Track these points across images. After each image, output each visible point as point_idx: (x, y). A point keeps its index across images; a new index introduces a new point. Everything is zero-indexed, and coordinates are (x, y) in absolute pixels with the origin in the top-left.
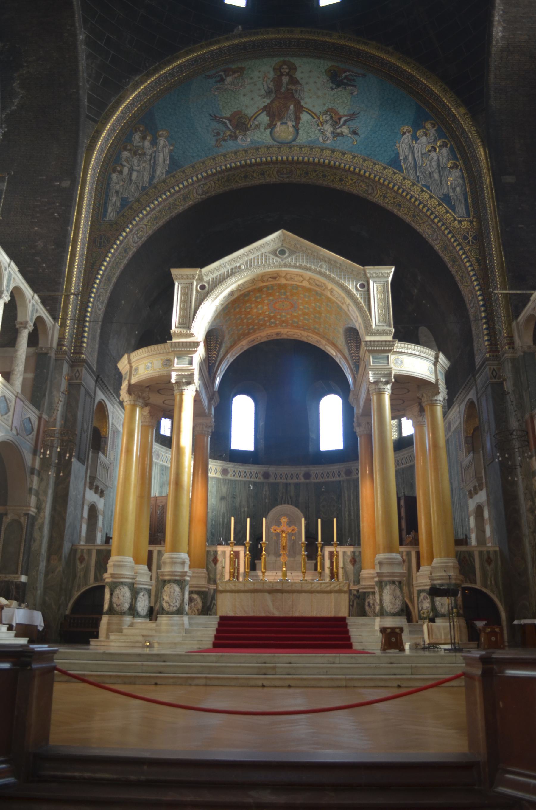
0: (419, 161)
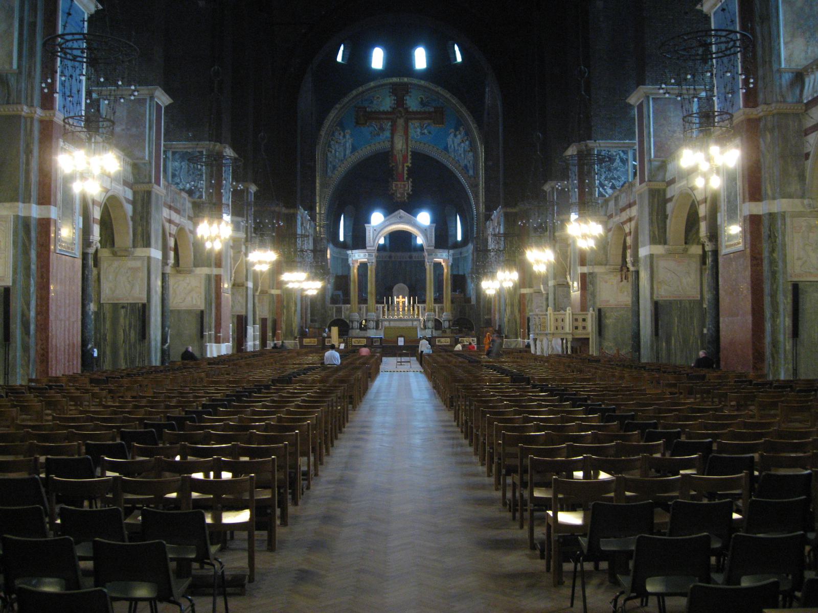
0: (456, 148)
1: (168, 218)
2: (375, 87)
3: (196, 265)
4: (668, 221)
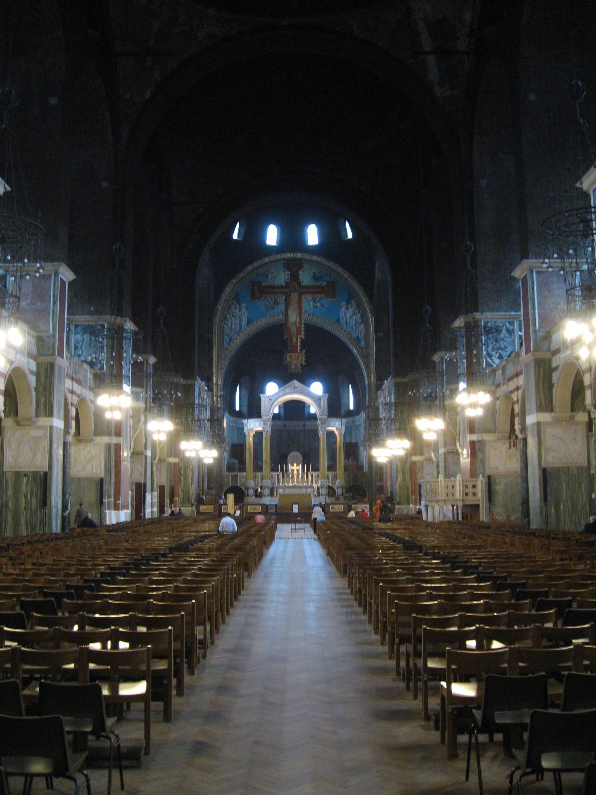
1: (70, 388)
2: (270, 262)
3: (95, 435)
4: (554, 390)
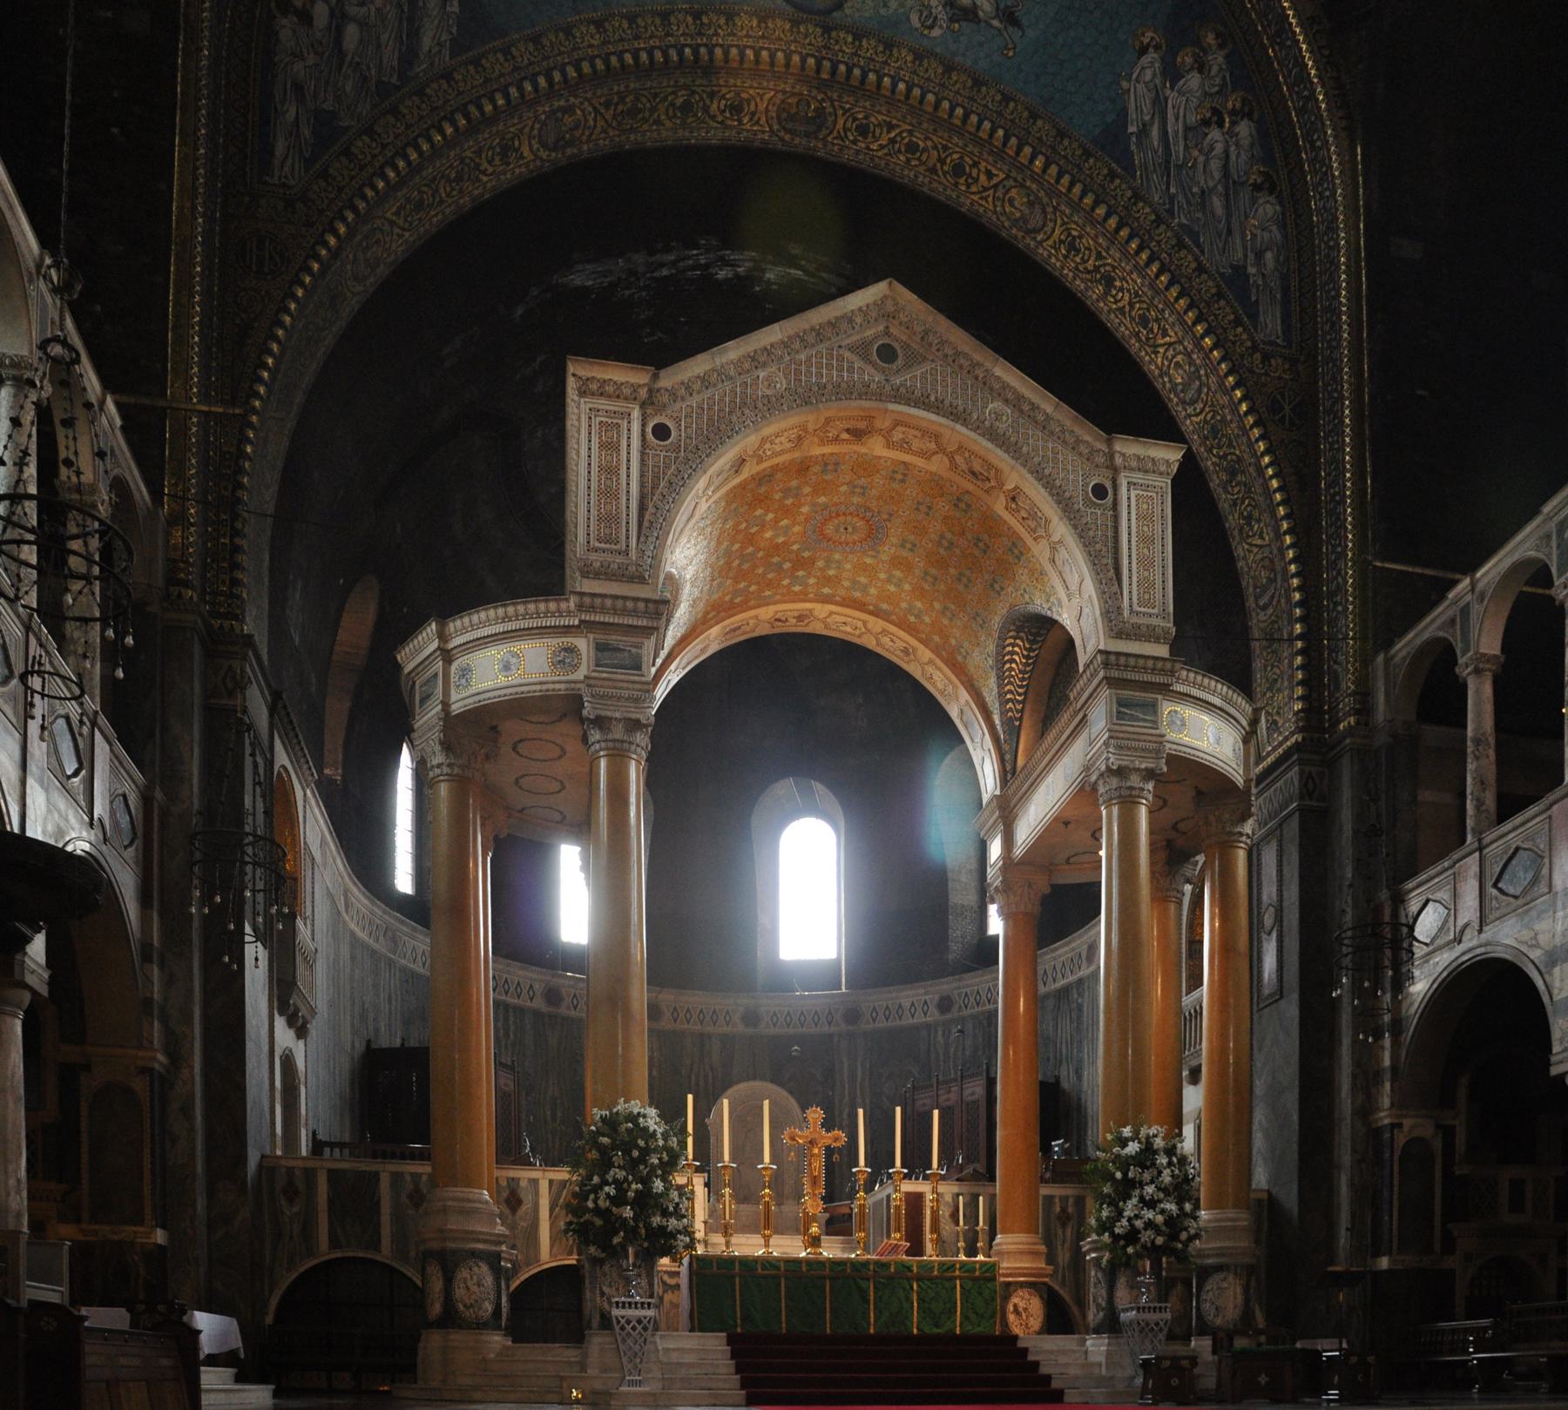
0: (1179, 150)
